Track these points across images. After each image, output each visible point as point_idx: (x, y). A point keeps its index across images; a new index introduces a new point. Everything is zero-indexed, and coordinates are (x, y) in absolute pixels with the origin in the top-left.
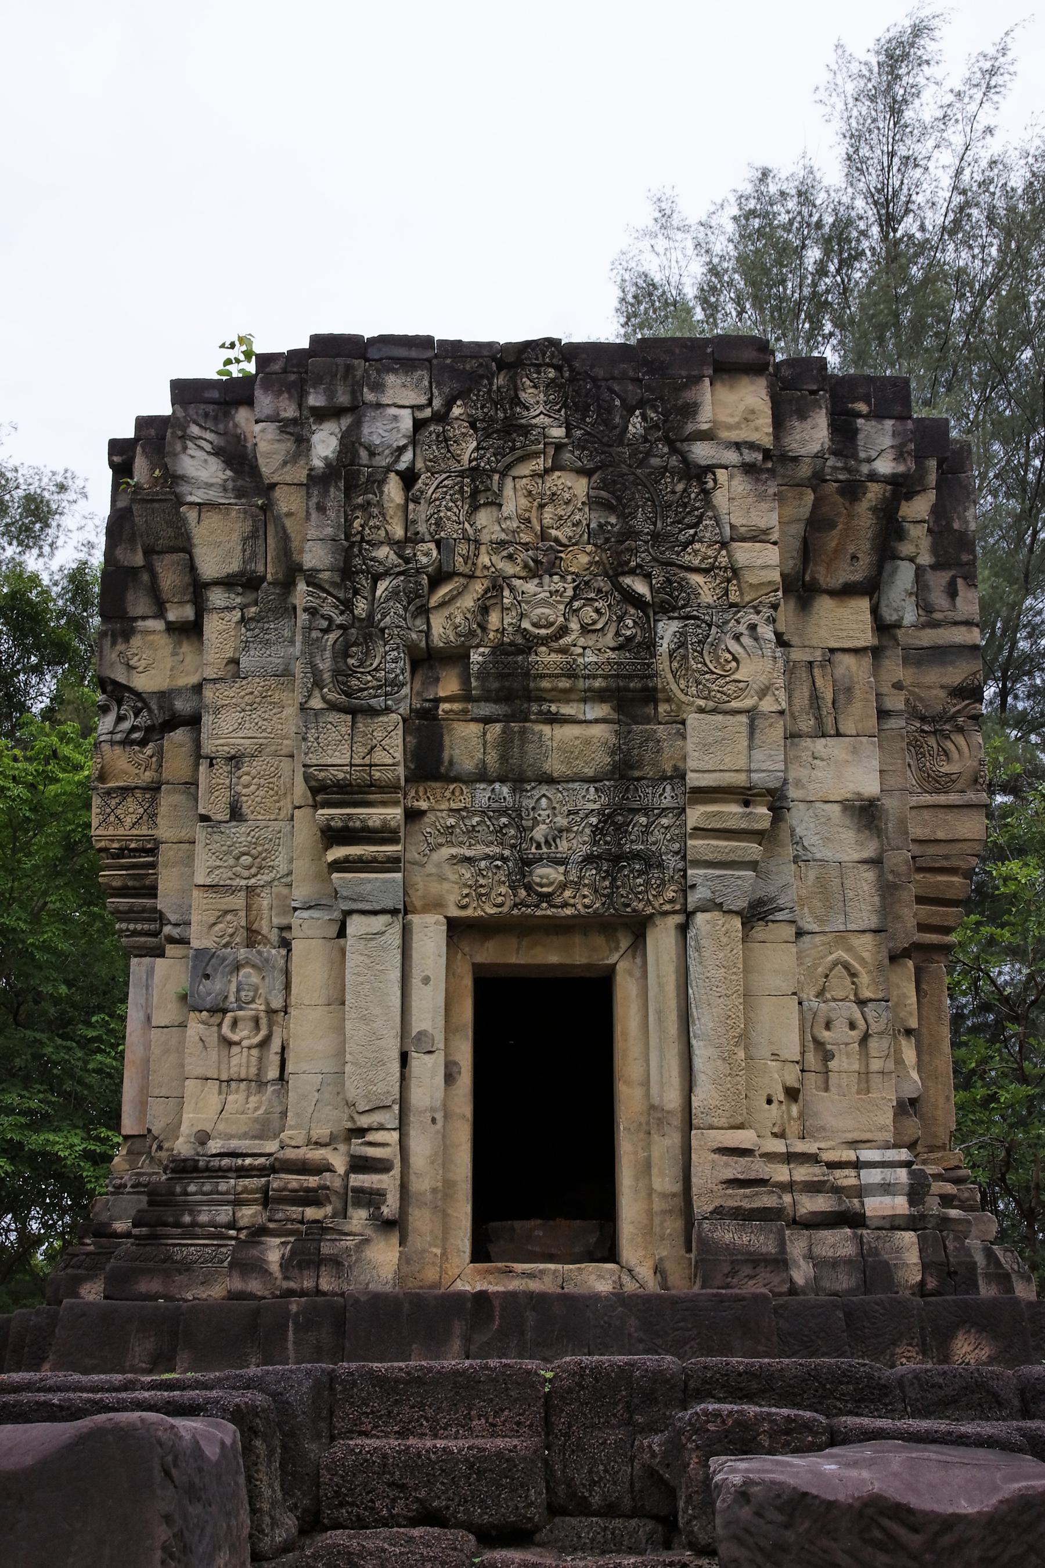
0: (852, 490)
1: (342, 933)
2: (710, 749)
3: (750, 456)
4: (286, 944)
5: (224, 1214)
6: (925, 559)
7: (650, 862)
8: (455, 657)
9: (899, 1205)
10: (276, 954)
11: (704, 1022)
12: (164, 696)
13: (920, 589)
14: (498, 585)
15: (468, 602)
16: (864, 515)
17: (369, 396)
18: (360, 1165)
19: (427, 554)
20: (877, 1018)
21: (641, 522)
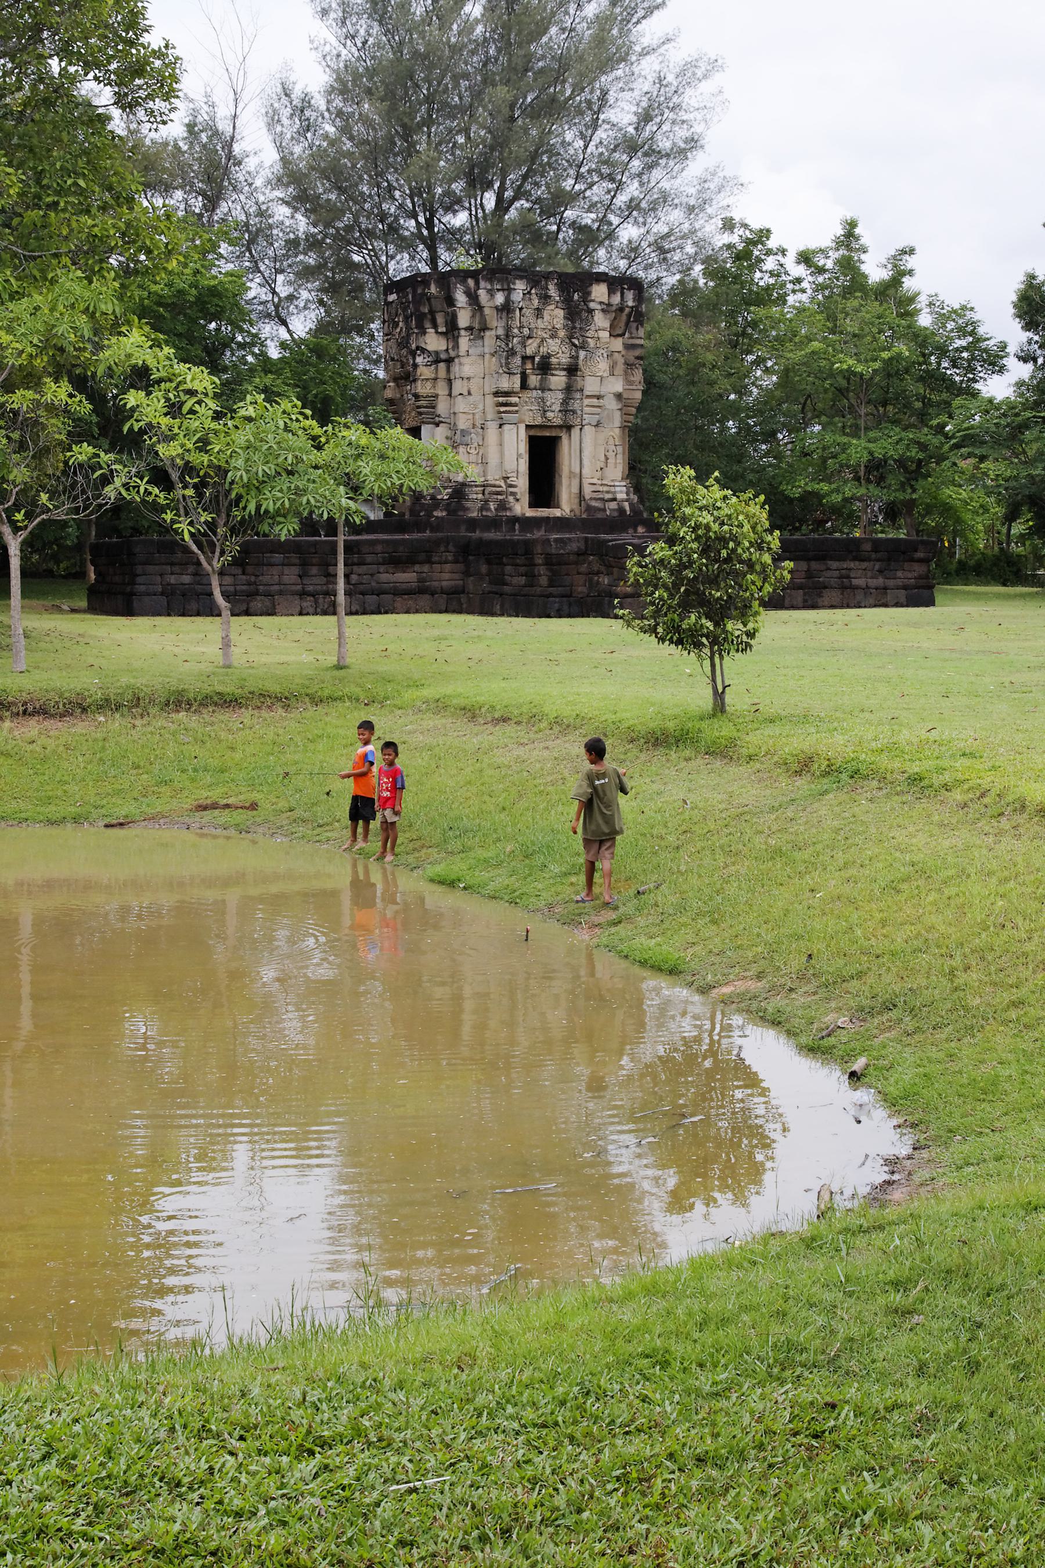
7: (574, 412)
8: (532, 358)
9: (624, 496)
12: (437, 353)
14: (543, 340)
15: (535, 345)
19: (526, 332)
21: (577, 325)
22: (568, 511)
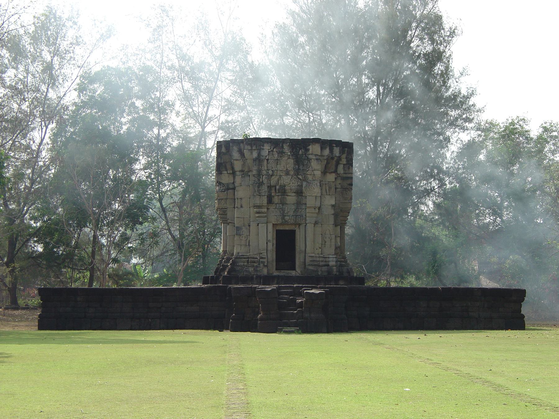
0: (333, 158)
1: (258, 225)
2: (311, 201)
3: (318, 157)
4: (249, 226)
5: (242, 264)
6: (345, 163)
10: (248, 227)
11: (308, 239)
12: (228, 184)
13: (344, 168)
16: (334, 162)
17: (262, 147)
18: (262, 258)
20: (333, 236)
22: (299, 272)
